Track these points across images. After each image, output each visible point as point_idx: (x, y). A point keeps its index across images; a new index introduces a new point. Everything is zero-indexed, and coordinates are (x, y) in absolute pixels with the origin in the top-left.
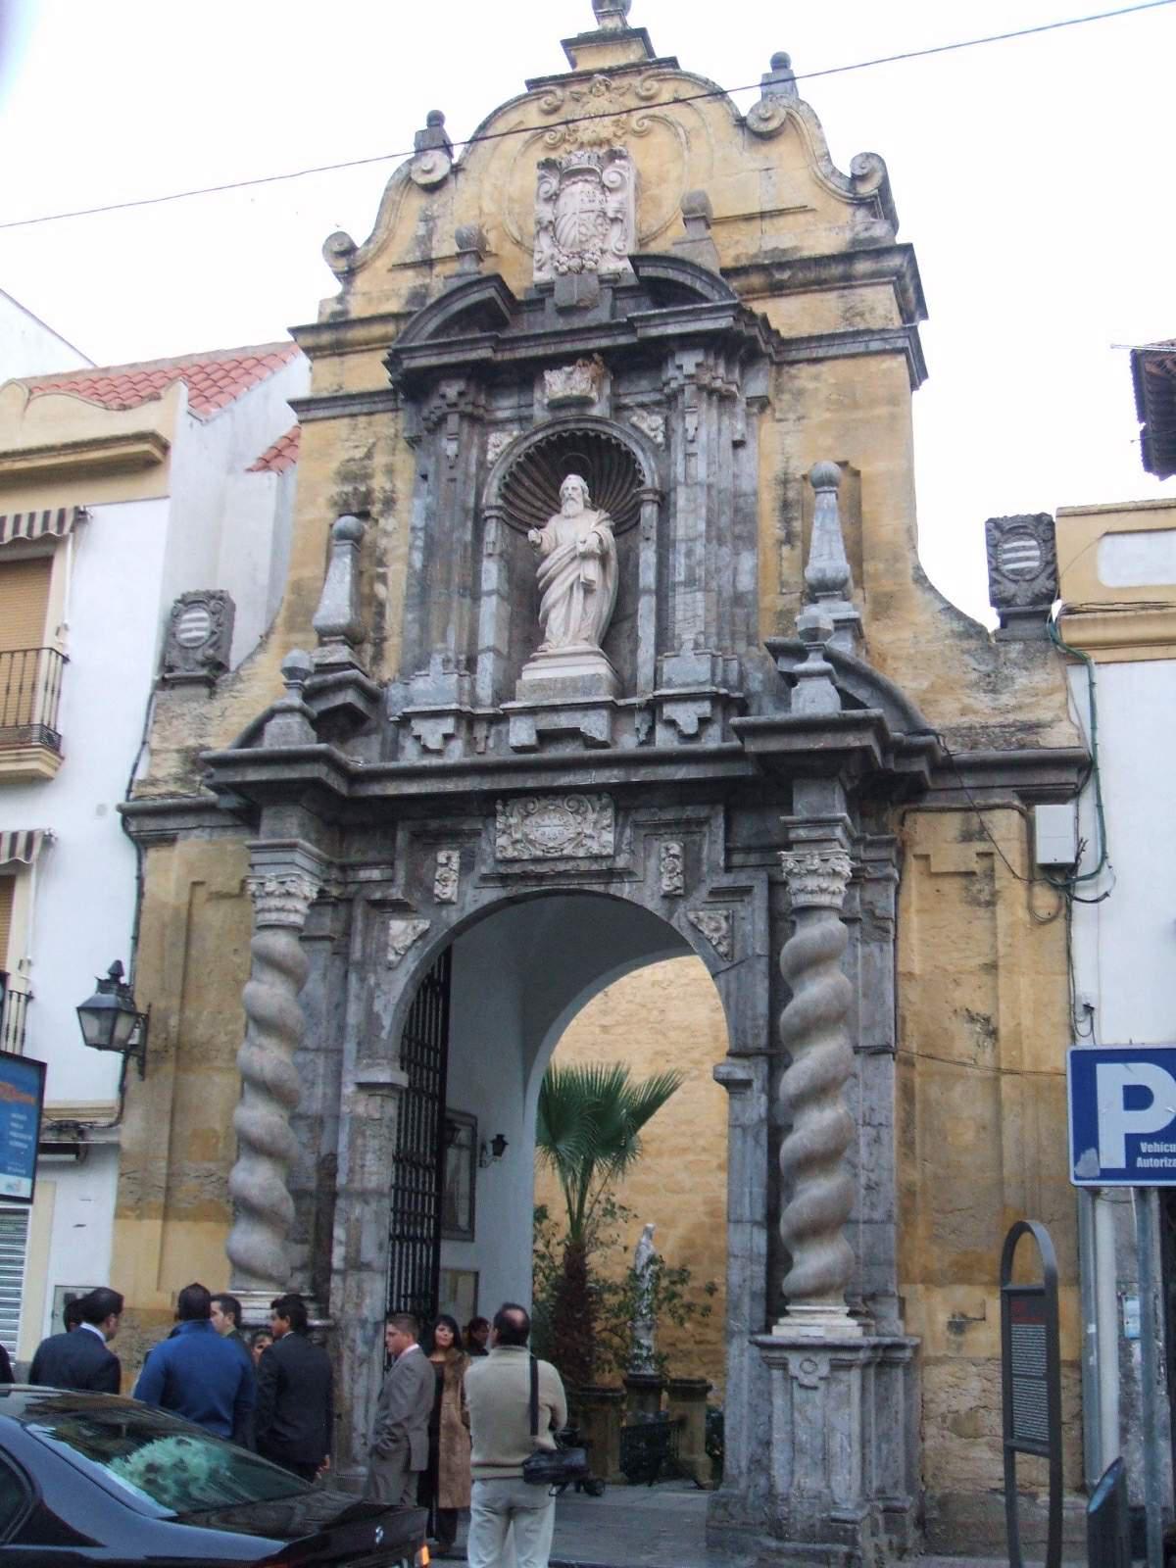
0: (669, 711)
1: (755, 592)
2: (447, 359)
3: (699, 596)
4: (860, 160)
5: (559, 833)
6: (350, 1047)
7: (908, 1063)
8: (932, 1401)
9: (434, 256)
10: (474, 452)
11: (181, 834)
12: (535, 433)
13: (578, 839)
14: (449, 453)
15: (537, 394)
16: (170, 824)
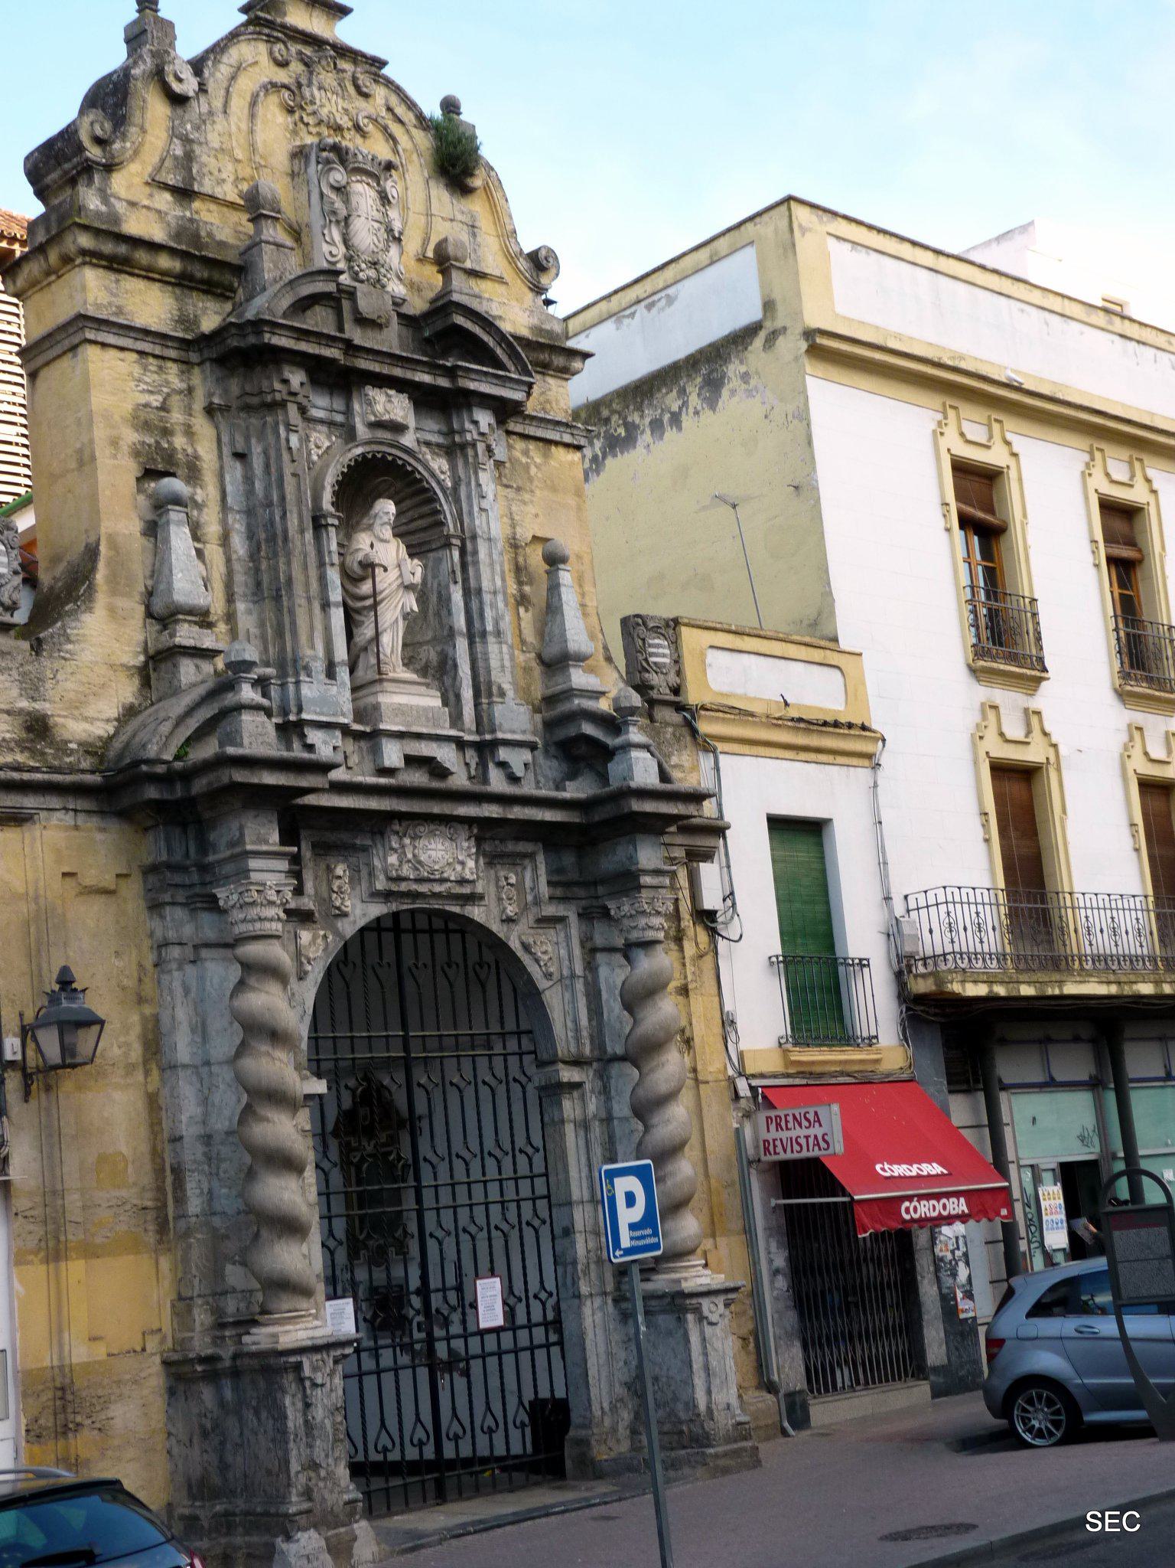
0: (503, 754)
2: (303, 346)
5: (442, 857)
9: (196, 188)
11: (43, 814)
16: (29, 802)
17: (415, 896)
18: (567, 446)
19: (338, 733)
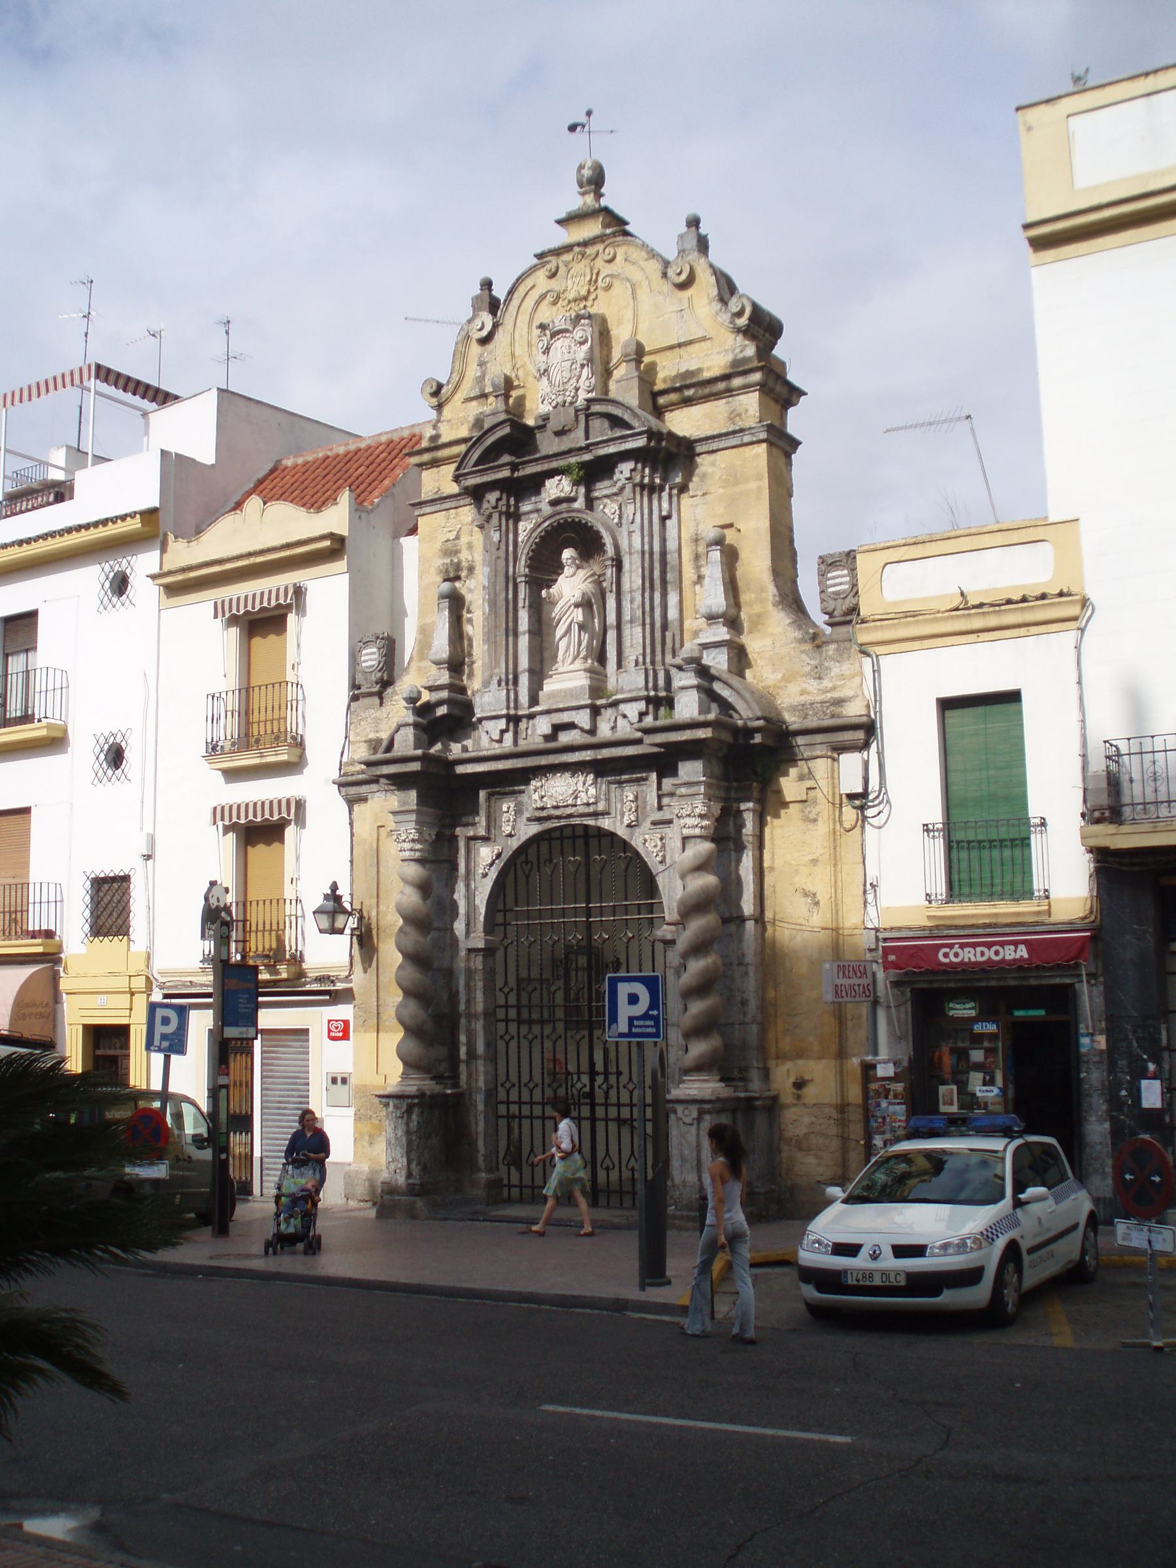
5: (561, 791)
15: (543, 495)
16: (363, 789)
17: (559, 817)
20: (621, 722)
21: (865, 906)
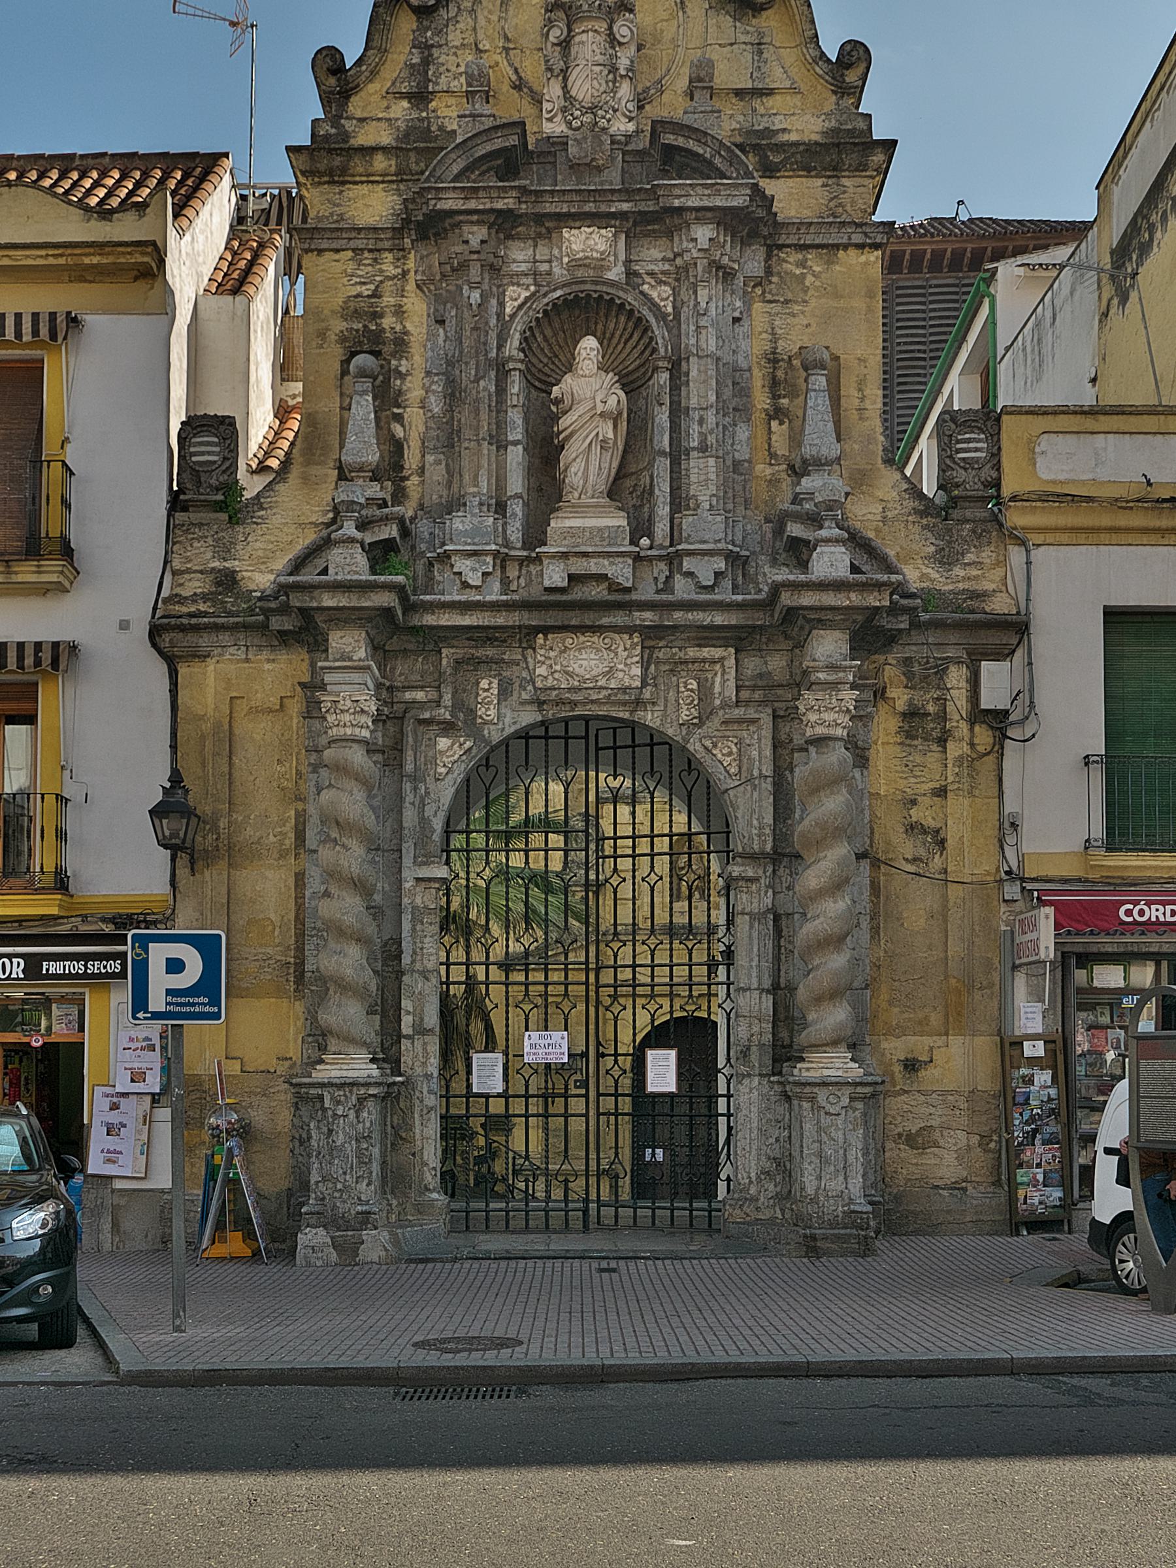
0: (687, 564)
1: (749, 461)
3: (712, 461)
4: (848, 48)
6: (408, 849)
7: (876, 863)
8: (891, 1123)
10: (494, 302)
12: (554, 290)
13: (610, 672)
14: (472, 301)
17: (575, 704)
18: (861, 247)
19: (489, 559)
20: (679, 582)
21: (1003, 849)
